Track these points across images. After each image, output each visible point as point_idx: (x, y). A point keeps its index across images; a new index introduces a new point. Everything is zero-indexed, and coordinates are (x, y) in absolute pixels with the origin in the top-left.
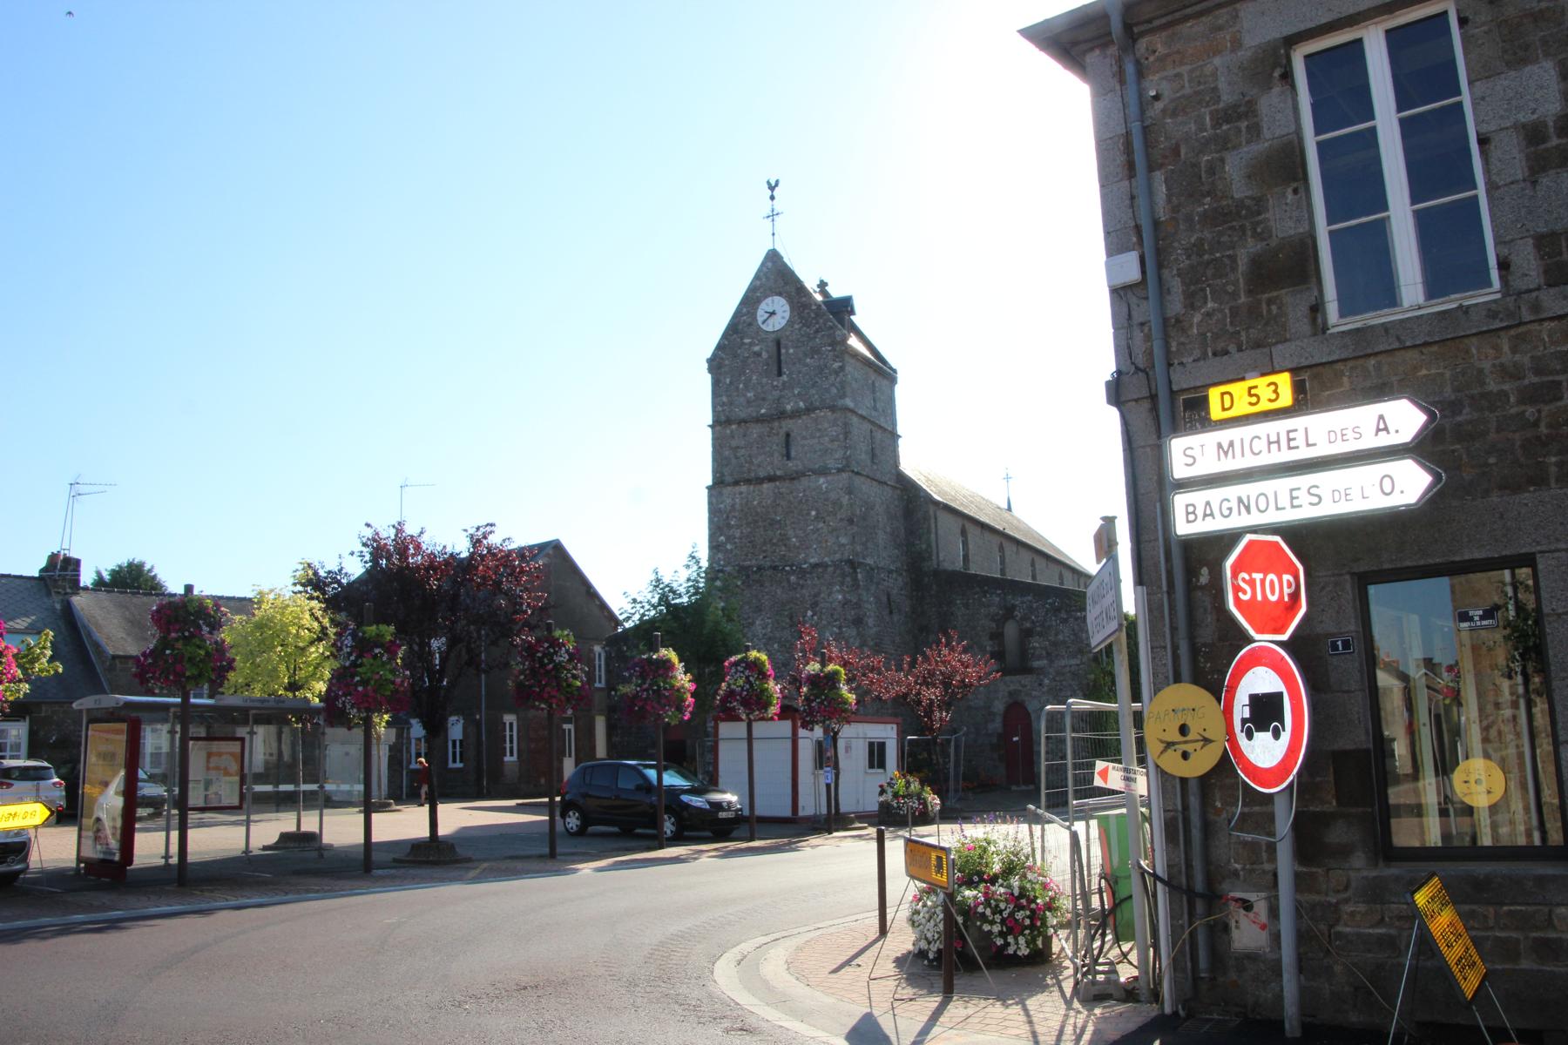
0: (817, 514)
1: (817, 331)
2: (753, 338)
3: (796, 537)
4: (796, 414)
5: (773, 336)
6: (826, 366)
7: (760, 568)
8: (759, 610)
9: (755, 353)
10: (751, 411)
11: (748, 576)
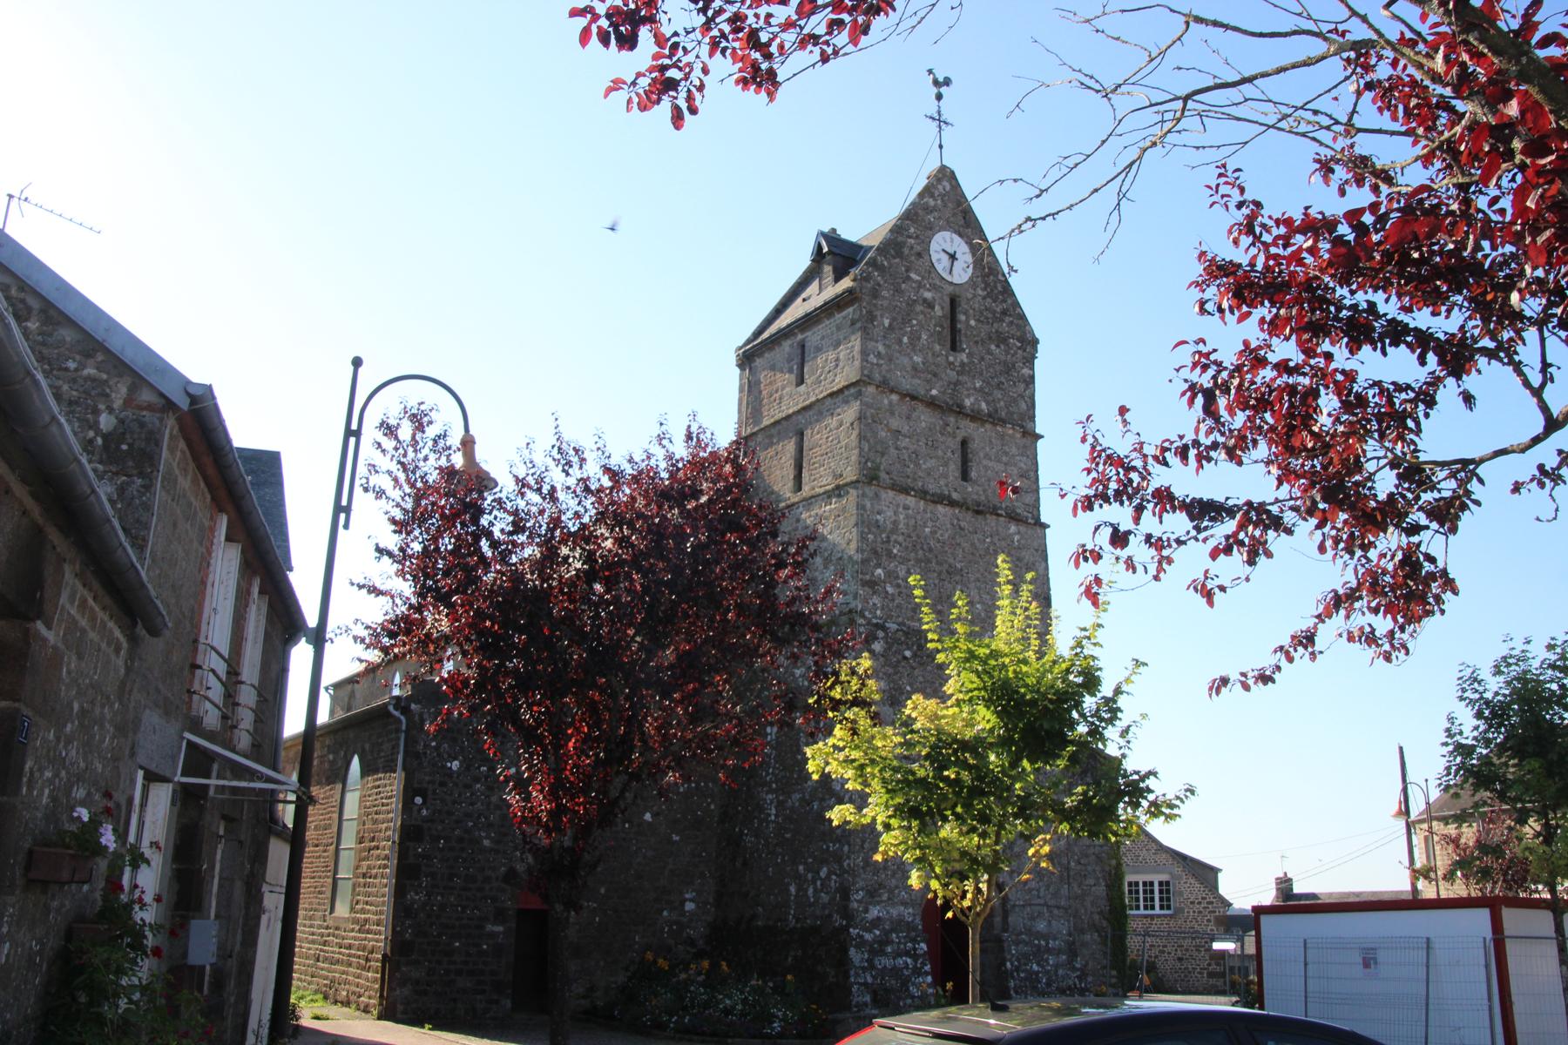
2: (923, 278)
4: (975, 417)
5: (951, 289)
9: (925, 300)
10: (907, 384)
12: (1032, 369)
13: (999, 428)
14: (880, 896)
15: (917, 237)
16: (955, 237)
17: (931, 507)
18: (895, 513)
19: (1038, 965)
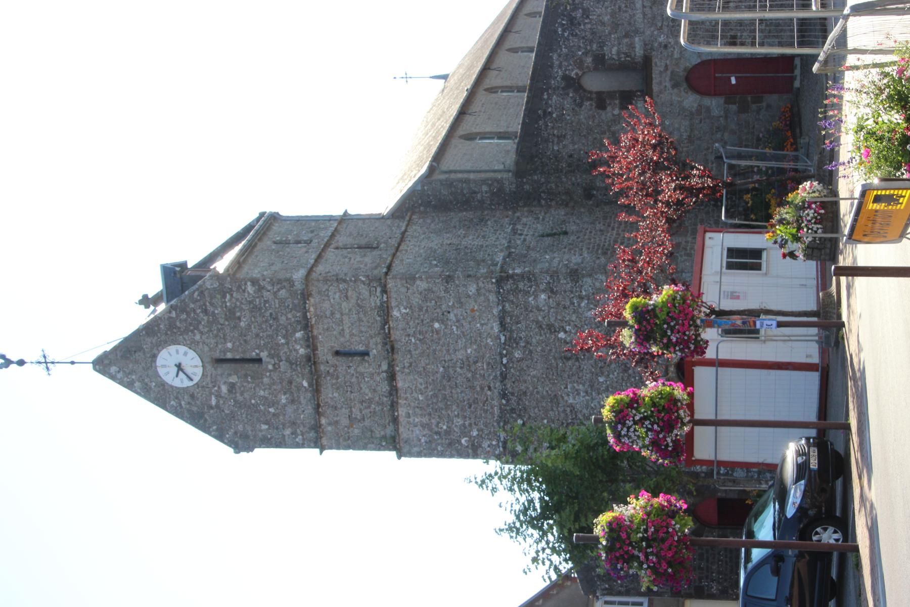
0: (438, 321)
1: (205, 311)
2: (211, 394)
3: (465, 348)
4: (311, 343)
5: (209, 367)
6: (250, 302)
7: (503, 395)
8: (555, 399)
9: (230, 391)
10: (305, 398)
11: (513, 410)
13: (313, 322)
15: (177, 398)
18: (416, 426)
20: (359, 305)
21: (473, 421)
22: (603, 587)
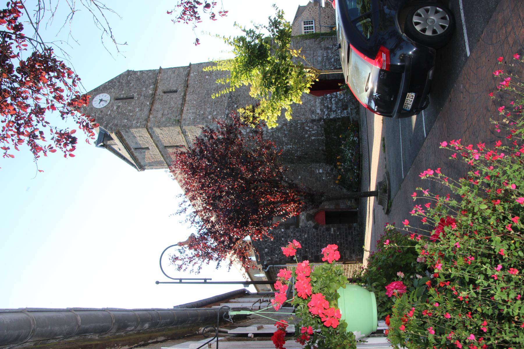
0: (208, 75)
2: (109, 110)
4: (155, 89)
5: (112, 101)
9: (117, 109)
11: (233, 102)
12: (138, 71)
13: (159, 81)
14: (313, 110)
15: (95, 113)
16: (94, 100)
17: (187, 102)
18: (190, 113)
19: (332, 59)
20: (178, 75)
21: (215, 109)
22: (268, 259)
